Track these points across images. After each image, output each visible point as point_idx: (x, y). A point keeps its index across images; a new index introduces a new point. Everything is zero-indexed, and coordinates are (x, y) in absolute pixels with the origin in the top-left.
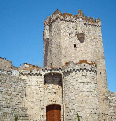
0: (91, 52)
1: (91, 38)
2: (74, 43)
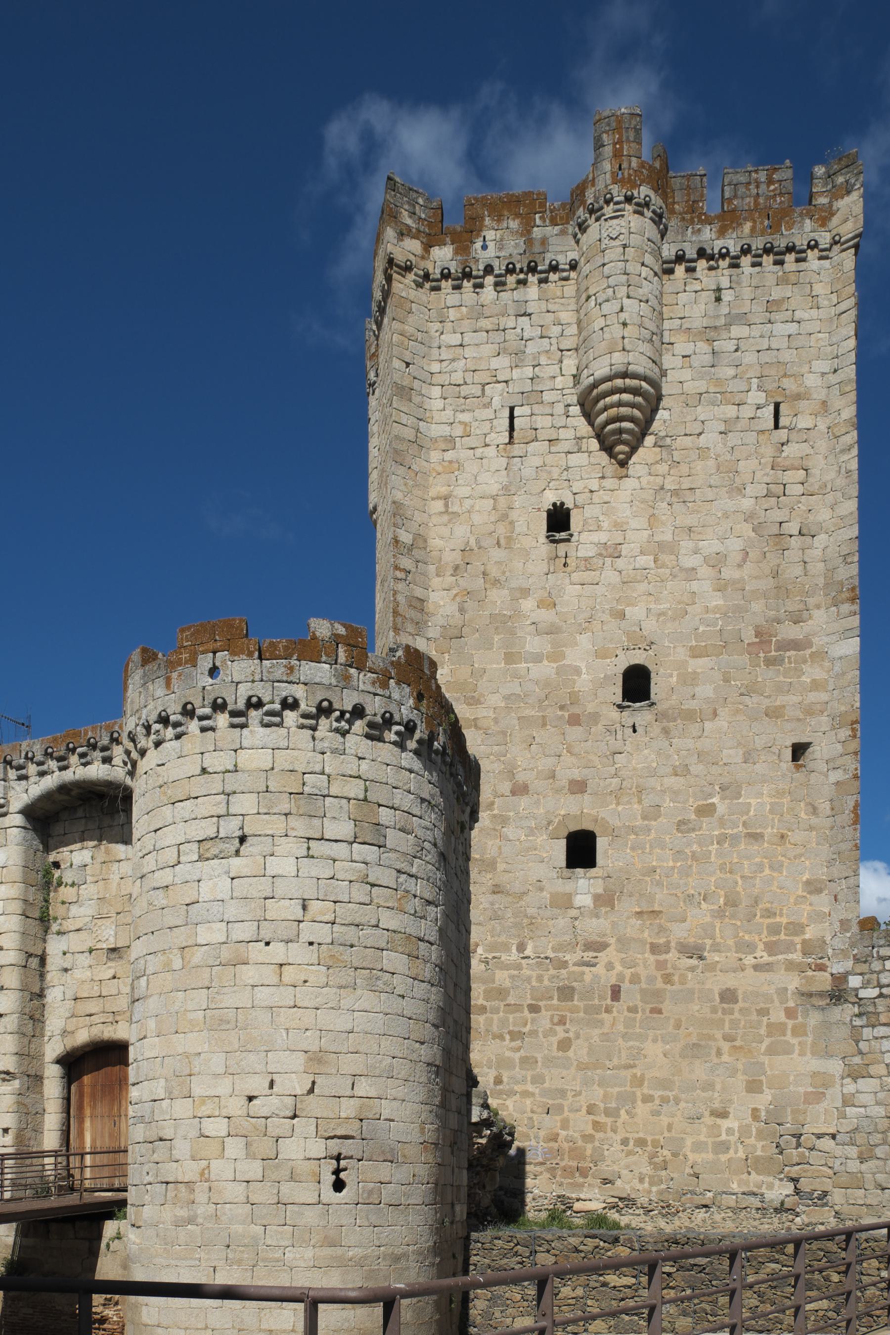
0: (717, 561)
1: (731, 411)
2: (550, 498)
